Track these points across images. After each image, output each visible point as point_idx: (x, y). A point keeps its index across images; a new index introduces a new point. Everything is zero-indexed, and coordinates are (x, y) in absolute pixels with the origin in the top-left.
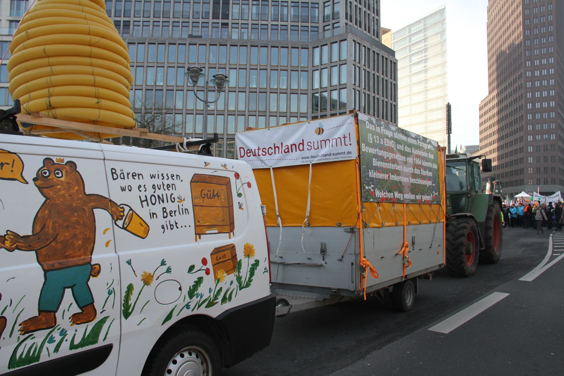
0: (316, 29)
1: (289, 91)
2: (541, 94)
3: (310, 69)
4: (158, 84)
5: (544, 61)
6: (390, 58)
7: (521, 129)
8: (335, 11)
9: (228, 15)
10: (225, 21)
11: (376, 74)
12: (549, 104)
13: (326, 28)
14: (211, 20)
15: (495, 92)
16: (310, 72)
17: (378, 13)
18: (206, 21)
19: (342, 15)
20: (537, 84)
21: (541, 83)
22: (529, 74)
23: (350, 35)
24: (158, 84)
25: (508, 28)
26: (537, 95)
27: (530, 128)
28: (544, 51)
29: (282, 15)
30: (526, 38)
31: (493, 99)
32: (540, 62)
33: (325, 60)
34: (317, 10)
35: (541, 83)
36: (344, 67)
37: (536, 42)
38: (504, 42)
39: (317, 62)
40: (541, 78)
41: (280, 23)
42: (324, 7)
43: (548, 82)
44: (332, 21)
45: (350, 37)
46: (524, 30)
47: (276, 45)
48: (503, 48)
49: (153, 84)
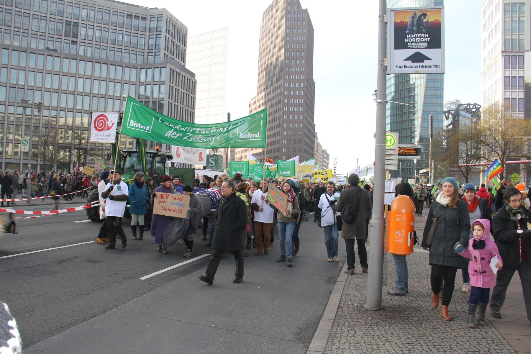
0: (142, 54)
1: (122, 98)
3: (138, 84)
4: (19, 83)
5: (297, 77)
6: (192, 79)
7: (278, 126)
8: (157, 43)
9: (77, 35)
10: (75, 40)
11: (183, 91)
12: (299, 109)
13: (150, 54)
14: (63, 37)
15: (263, 94)
16: (138, 86)
17: (185, 44)
18: (60, 37)
19: (162, 47)
20: (292, 93)
21: (294, 93)
22: (286, 85)
23: (168, 64)
24: (19, 83)
25: (275, 47)
26: (292, 101)
27: (285, 125)
28: (298, 69)
29: (118, 41)
30: (286, 58)
31: (260, 99)
32: (295, 77)
33: (149, 79)
34: (144, 39)
35: (294, 93)
36: (162, 86)
37: (293, 62)
38: (271, 57)
39: (143, 79)
40: (295, 89)
41: (116, 46)
42: (149, 38)
43: (299, 93)
44: (154, 51)
45: (169, 66)
46: (285, 51)
47: (114, 63)
49: (15, 83)
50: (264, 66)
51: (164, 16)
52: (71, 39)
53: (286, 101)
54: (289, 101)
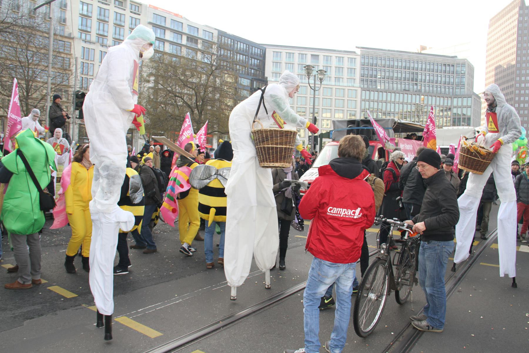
2: (524, 99)
20: (522, 92)
21: (525, 92)
22: (518, 85)
33: (460, 104)
35: (525, 92)
37: (524, 65)
48: (501, 63)
50: (493, 67)
51: (466, 64)
52: (414, 82)
53: (517, 99)
54: (519, 99)
